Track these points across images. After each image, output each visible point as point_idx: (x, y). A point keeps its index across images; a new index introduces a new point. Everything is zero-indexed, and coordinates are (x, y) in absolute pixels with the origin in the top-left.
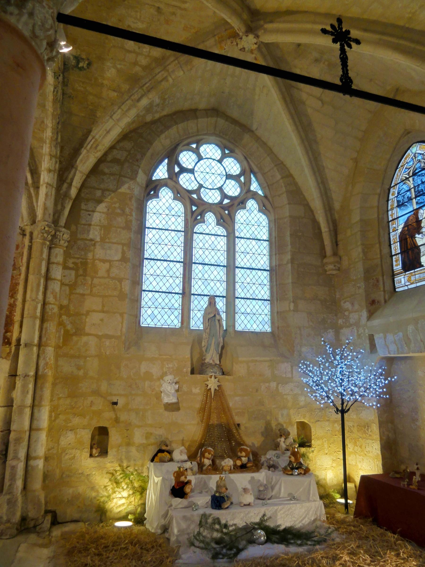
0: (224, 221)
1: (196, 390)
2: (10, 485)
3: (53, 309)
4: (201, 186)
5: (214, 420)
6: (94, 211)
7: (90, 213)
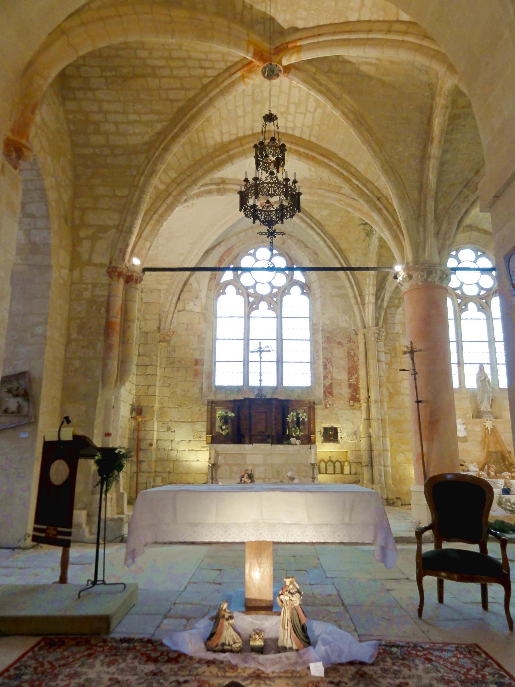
0: (483, 308)
1: (478, 429)
2: (380, 479)
3: (384, 379)
4: (462, 283)
5: (492, 449)
6: (395, 314)
7: (393, 315)
